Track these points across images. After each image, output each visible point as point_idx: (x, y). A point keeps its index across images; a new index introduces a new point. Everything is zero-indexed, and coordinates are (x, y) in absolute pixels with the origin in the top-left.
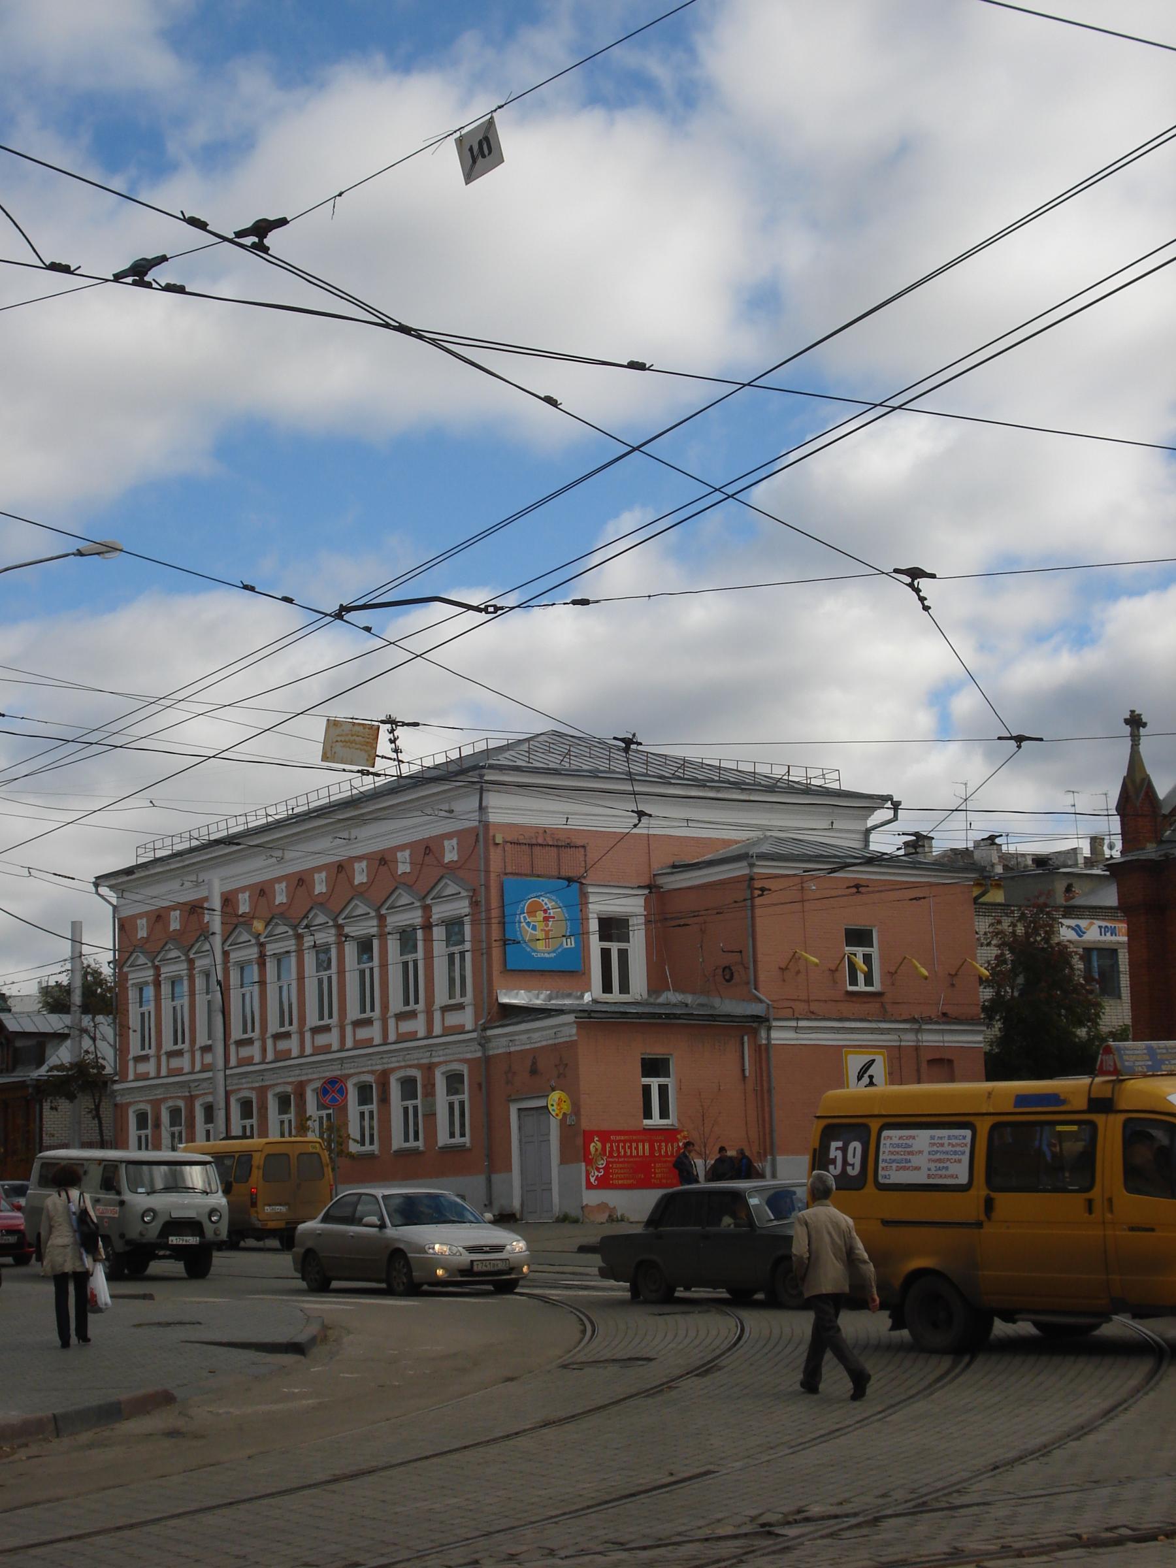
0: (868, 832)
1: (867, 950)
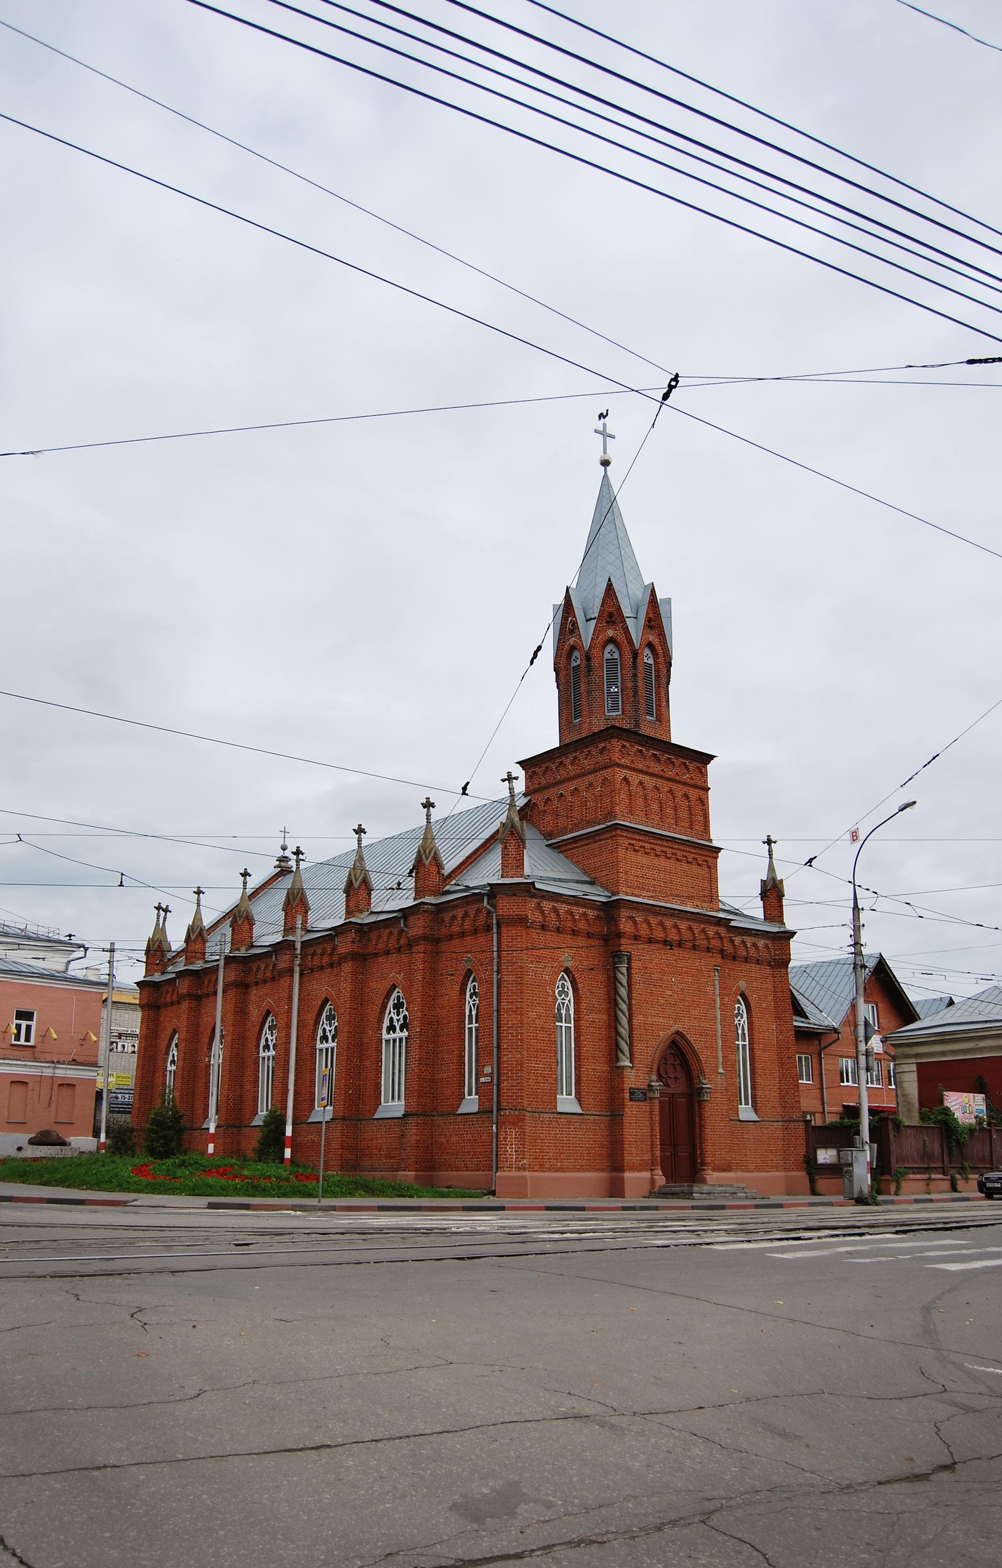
0: (69, 962)
1: (29, 1023)
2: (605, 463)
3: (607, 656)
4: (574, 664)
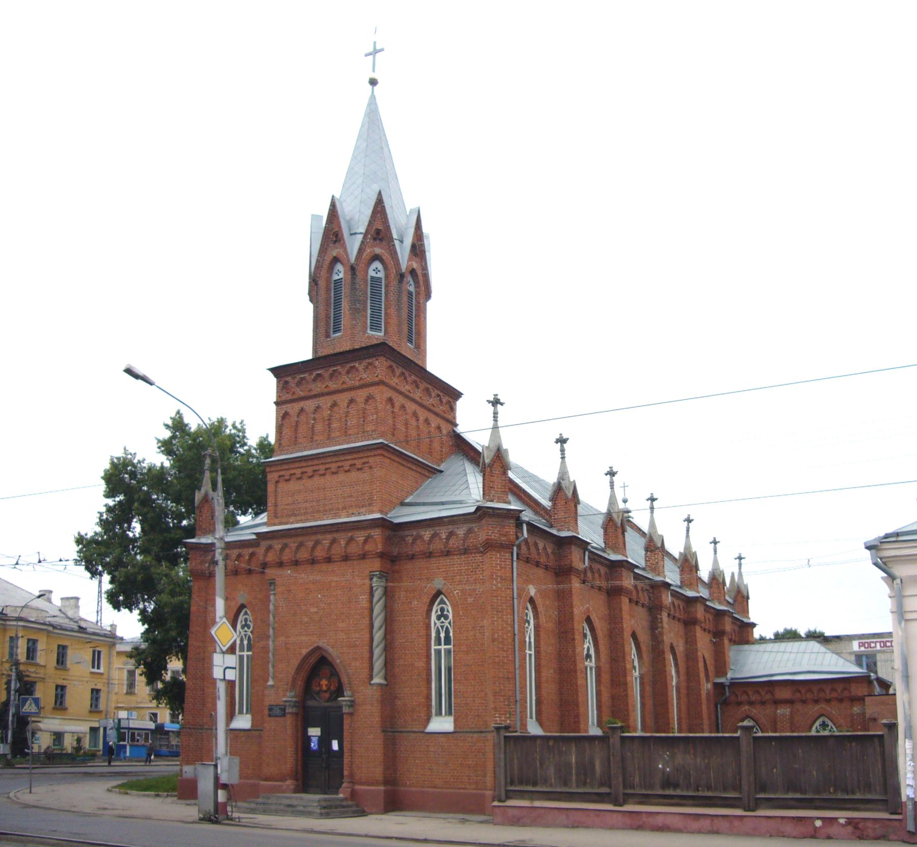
2: (373, 82)
3: (371, 273)
4: (336, 277)
